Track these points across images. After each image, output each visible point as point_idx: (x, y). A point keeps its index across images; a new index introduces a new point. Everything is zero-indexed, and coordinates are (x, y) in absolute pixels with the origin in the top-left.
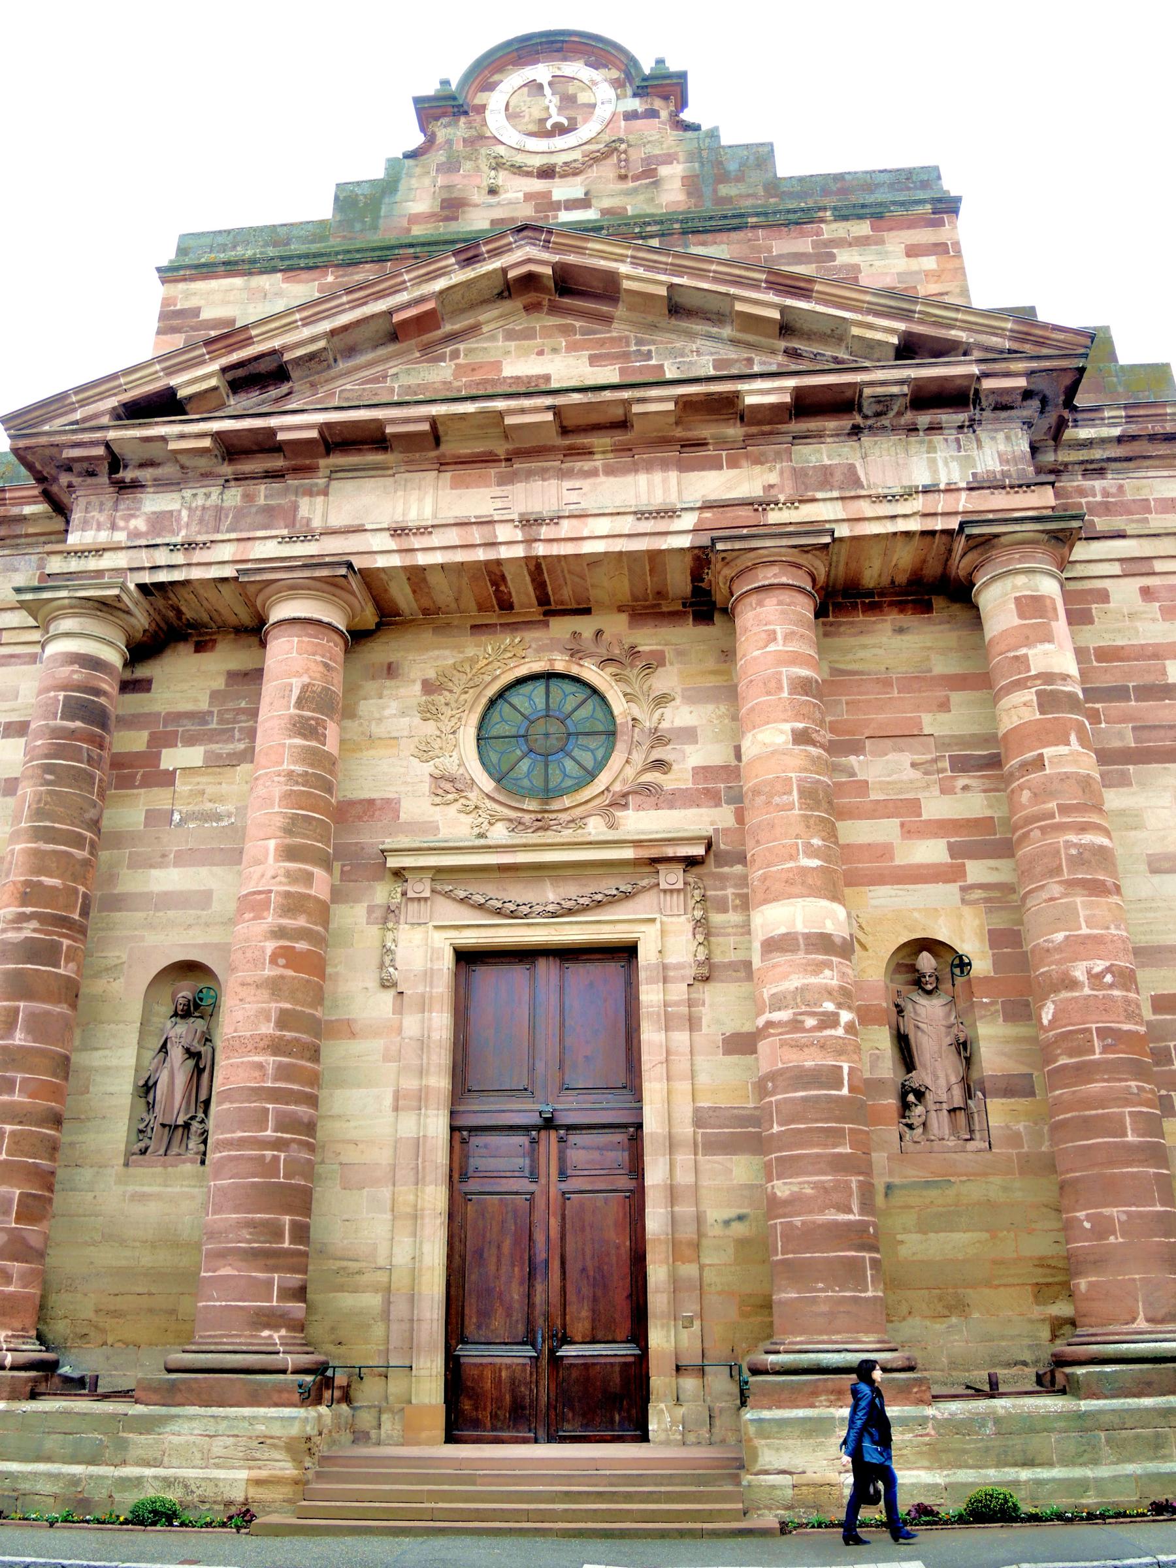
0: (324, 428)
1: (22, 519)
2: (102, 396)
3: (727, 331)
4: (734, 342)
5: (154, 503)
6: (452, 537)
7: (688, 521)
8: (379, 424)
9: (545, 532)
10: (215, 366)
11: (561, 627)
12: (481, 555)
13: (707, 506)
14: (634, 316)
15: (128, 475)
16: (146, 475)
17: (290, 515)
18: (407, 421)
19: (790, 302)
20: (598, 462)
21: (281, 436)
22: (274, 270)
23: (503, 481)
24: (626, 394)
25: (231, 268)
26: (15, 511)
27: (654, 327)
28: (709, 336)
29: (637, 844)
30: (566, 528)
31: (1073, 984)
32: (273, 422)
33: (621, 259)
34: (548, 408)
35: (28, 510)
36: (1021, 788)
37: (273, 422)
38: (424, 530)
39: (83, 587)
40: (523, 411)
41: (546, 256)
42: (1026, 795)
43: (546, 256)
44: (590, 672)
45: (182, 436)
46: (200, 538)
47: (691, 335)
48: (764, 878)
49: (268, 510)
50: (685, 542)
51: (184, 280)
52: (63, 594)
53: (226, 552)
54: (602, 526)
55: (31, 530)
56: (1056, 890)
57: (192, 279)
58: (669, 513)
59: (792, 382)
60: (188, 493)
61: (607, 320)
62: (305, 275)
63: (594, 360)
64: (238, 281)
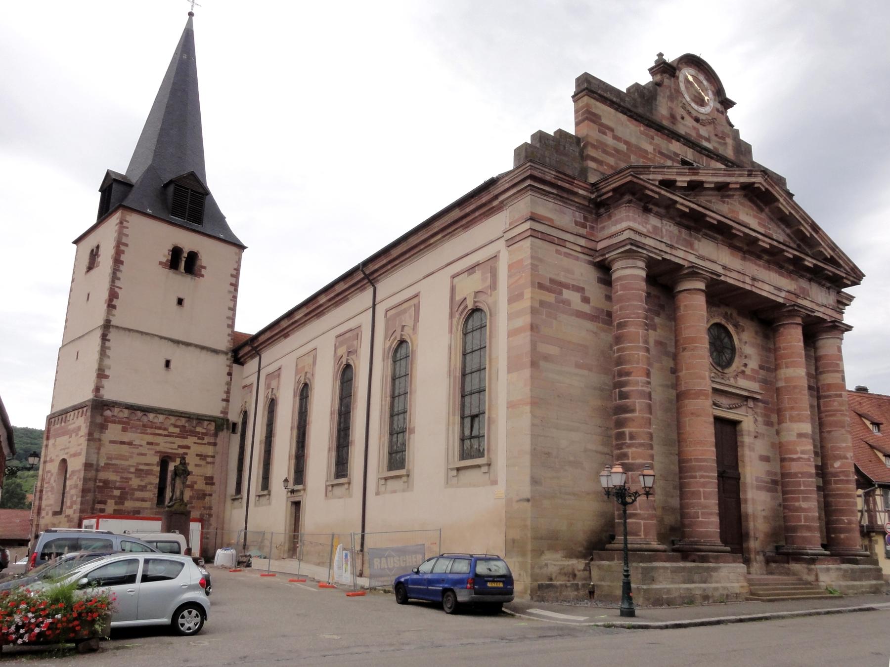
0: (719, 221)
1: (576, 194)
2: (659, 173)
3: (788, 231)
4: (788, 235)
5: (654, 221)
6: (741, 277)
7: (783, 294)
8: (731, 227)
9: (756, 284)
10: (688, 179)
11: (723, 310)
12: (741, 285)
13: (788, 292)
14: (769, 214)
15: (651, 206)
16: (655, 209)
17: (691, 246)
18: (738, 230)
19: (813, 233)
20: (761, 263)
21: (708, 219)
22: (625, 114)
23: (744, 259)
24: (784, 248)
25: (612, 104)
26: (576, 190)
27: (771, 219)
28: (783, 230)
29: (749, 391)
30: (759, 285)
31: (847, 458)
32: (708, 212)
33: (781, 196)
34: (770, 244)
35: (581, 192)
36: (834, 401)
37: (708, 212)
38: (730, 270)
39: (651, 252)
40: (764, 241)
41: (765, 184)
42: (836, 404)
43: (765, 184)
44: (731, 328)
45: (682, 204)
46: (676, 245)
47: (779, 226)
48: (799, 415)
49: (685, 240)
50: (781, 301)
51: (594, 98)
52: (645, 252)
53: (681, 254)
54: (767, 287)
55: (576, 200)
56: (844, 432)
57: (597, 100)
58: (780, 289)
59: (815, 262)
60: (664, 222)
61: (762, 210)
62: (635, 122)
63: (759, 224)
64: (612, 111)
